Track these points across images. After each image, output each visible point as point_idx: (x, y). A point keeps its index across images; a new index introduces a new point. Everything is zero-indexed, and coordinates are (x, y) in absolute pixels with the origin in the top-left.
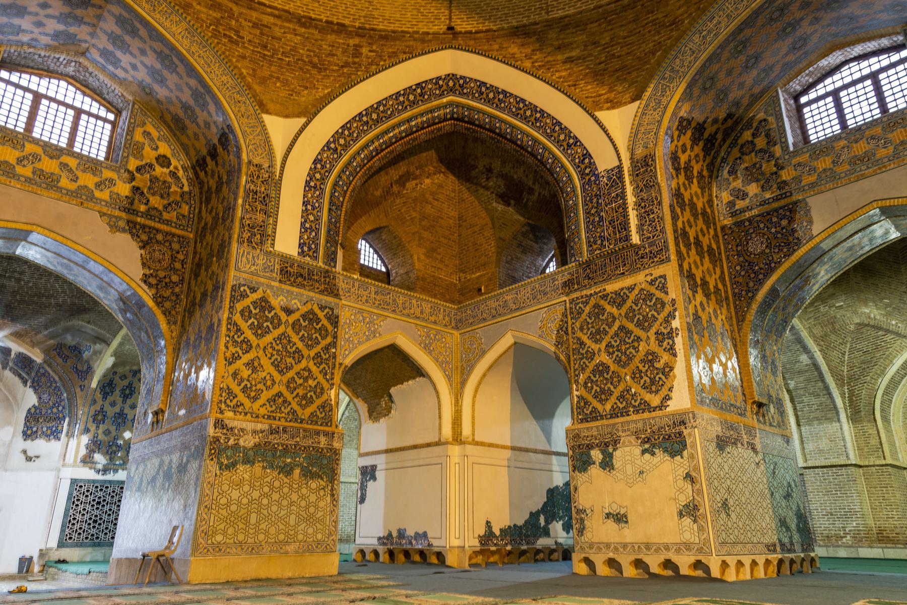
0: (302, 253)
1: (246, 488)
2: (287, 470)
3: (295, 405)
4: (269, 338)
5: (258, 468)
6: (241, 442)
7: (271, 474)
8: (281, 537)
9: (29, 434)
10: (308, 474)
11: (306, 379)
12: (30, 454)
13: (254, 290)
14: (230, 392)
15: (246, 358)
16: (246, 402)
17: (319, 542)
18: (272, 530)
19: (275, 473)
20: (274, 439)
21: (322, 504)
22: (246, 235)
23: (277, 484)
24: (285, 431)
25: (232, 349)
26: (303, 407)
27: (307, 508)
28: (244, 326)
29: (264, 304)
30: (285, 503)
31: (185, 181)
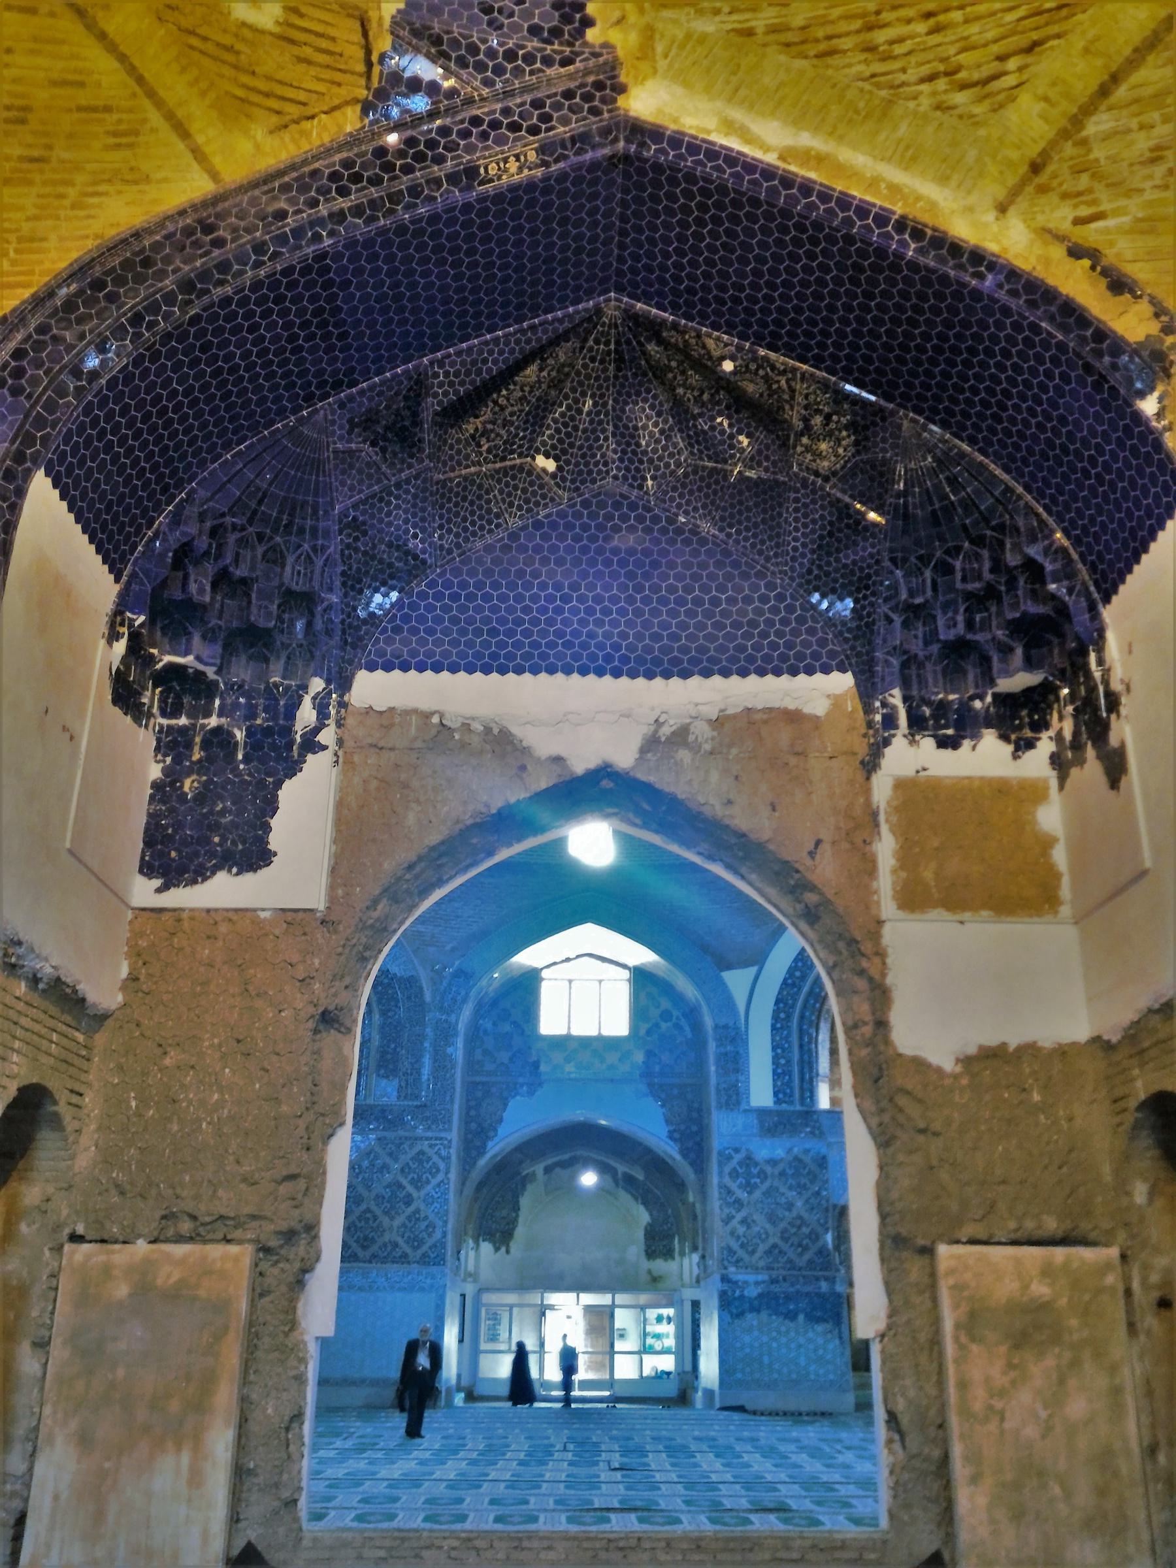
0: (778, 1101)
1: (756, 1333)
2: (791, 1316)
3: (791, 1254)
4: (757, 1194)
5: (764, 1315)
6: (746, 1293)
7: (777, 1321)
8: (794, 1376)
9: (651, 1254)
10: (812, 1319)
11: (799, 1227)
12: (655, 1274)
13: (737, 1150)
14: (731, 1252)
15: (739, 1217)
16: (746, 1257)
17: (832, 1382)
18: (785, 1370)
19: (781, 1319)
20: (776, 1288)
21: (831, 1346)
22: (723, 1101)
23: (783, 1329)
24: (785, 1280)
25: (726, 1211)
26: (801, 1255)
27: (815, 1350)
28: (734, 1186)
29: (749, 1161)
30: (793, 1346)
31: (687, 1029)
